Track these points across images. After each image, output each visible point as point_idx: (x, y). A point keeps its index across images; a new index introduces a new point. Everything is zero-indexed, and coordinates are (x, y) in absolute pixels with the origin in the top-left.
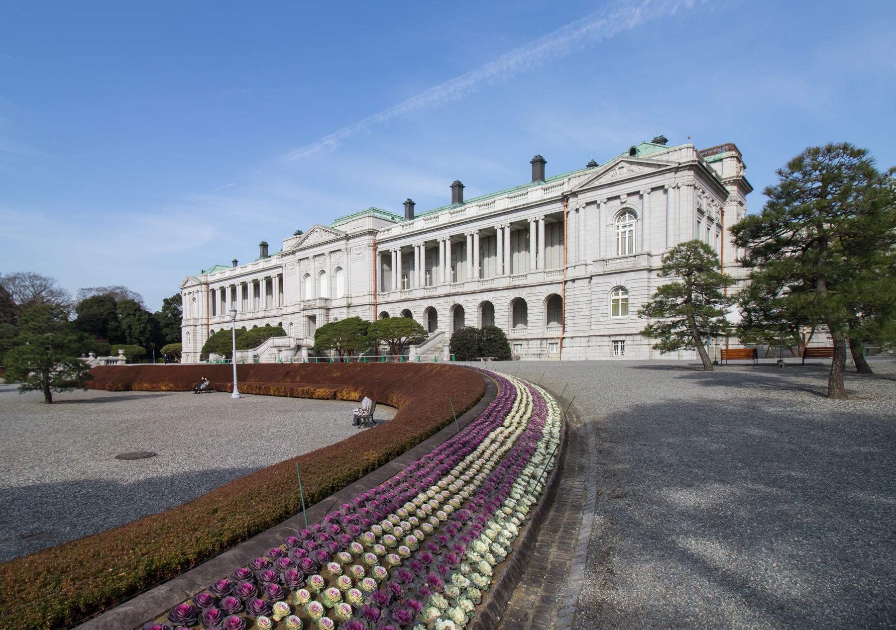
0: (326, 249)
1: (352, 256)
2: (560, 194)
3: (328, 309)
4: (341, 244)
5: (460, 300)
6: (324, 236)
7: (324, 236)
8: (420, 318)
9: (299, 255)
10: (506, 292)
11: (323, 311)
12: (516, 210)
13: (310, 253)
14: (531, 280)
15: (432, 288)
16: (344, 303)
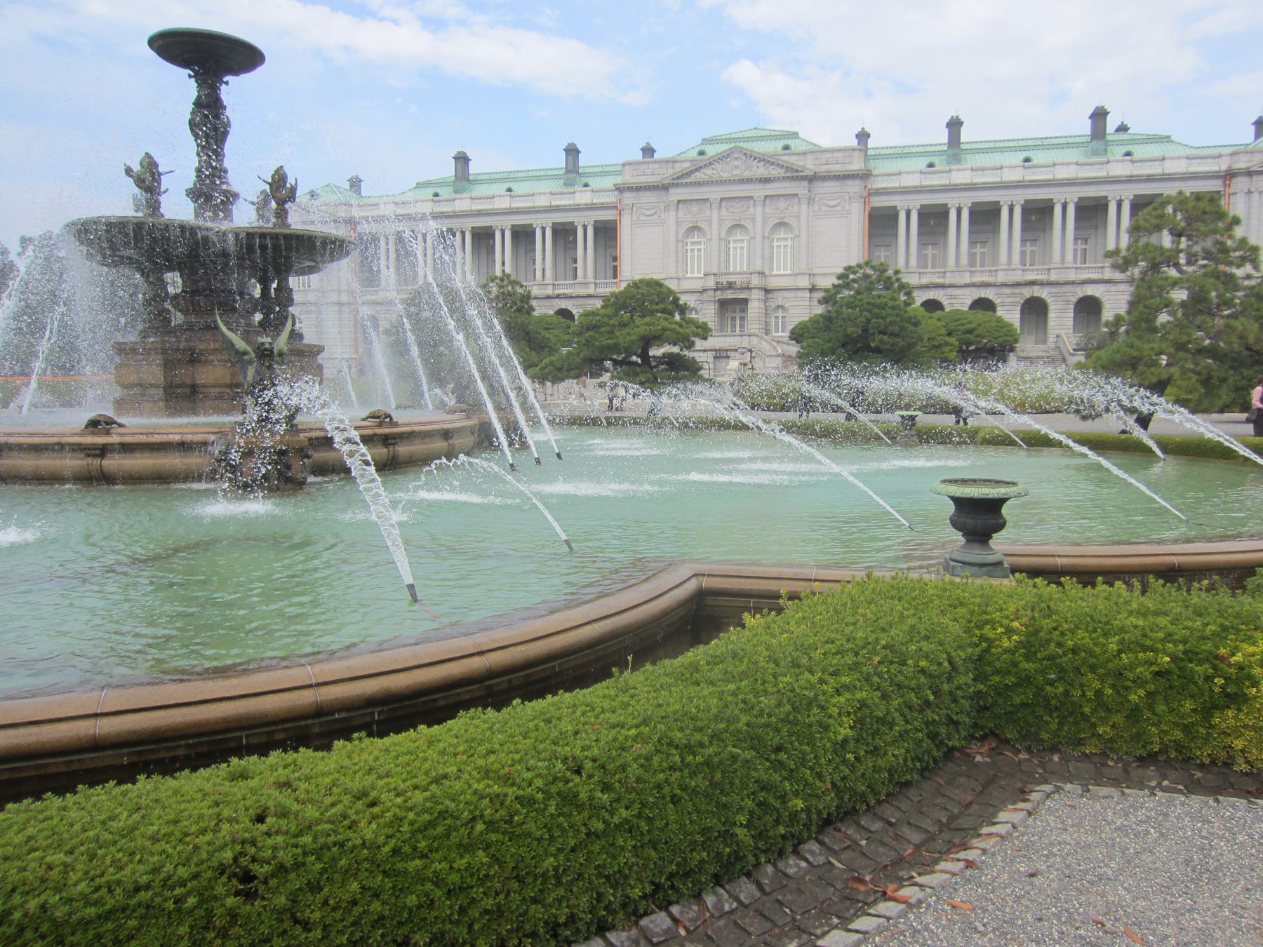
0: (758, 191)
1: (816, 208)
2: (1224, 168)
3: (767, 291)
4: (800, 188)
5: (1043, 293)
6: (755, 169)
7: (755, 169)
8: (1010, 314)
9: (676, 194)
10: (967, 291)
11: (761, 295)
12: (1150, 179)
13: (714, 193)
14: (957, 280)
15: (983, 272)
16: (804, 282)
